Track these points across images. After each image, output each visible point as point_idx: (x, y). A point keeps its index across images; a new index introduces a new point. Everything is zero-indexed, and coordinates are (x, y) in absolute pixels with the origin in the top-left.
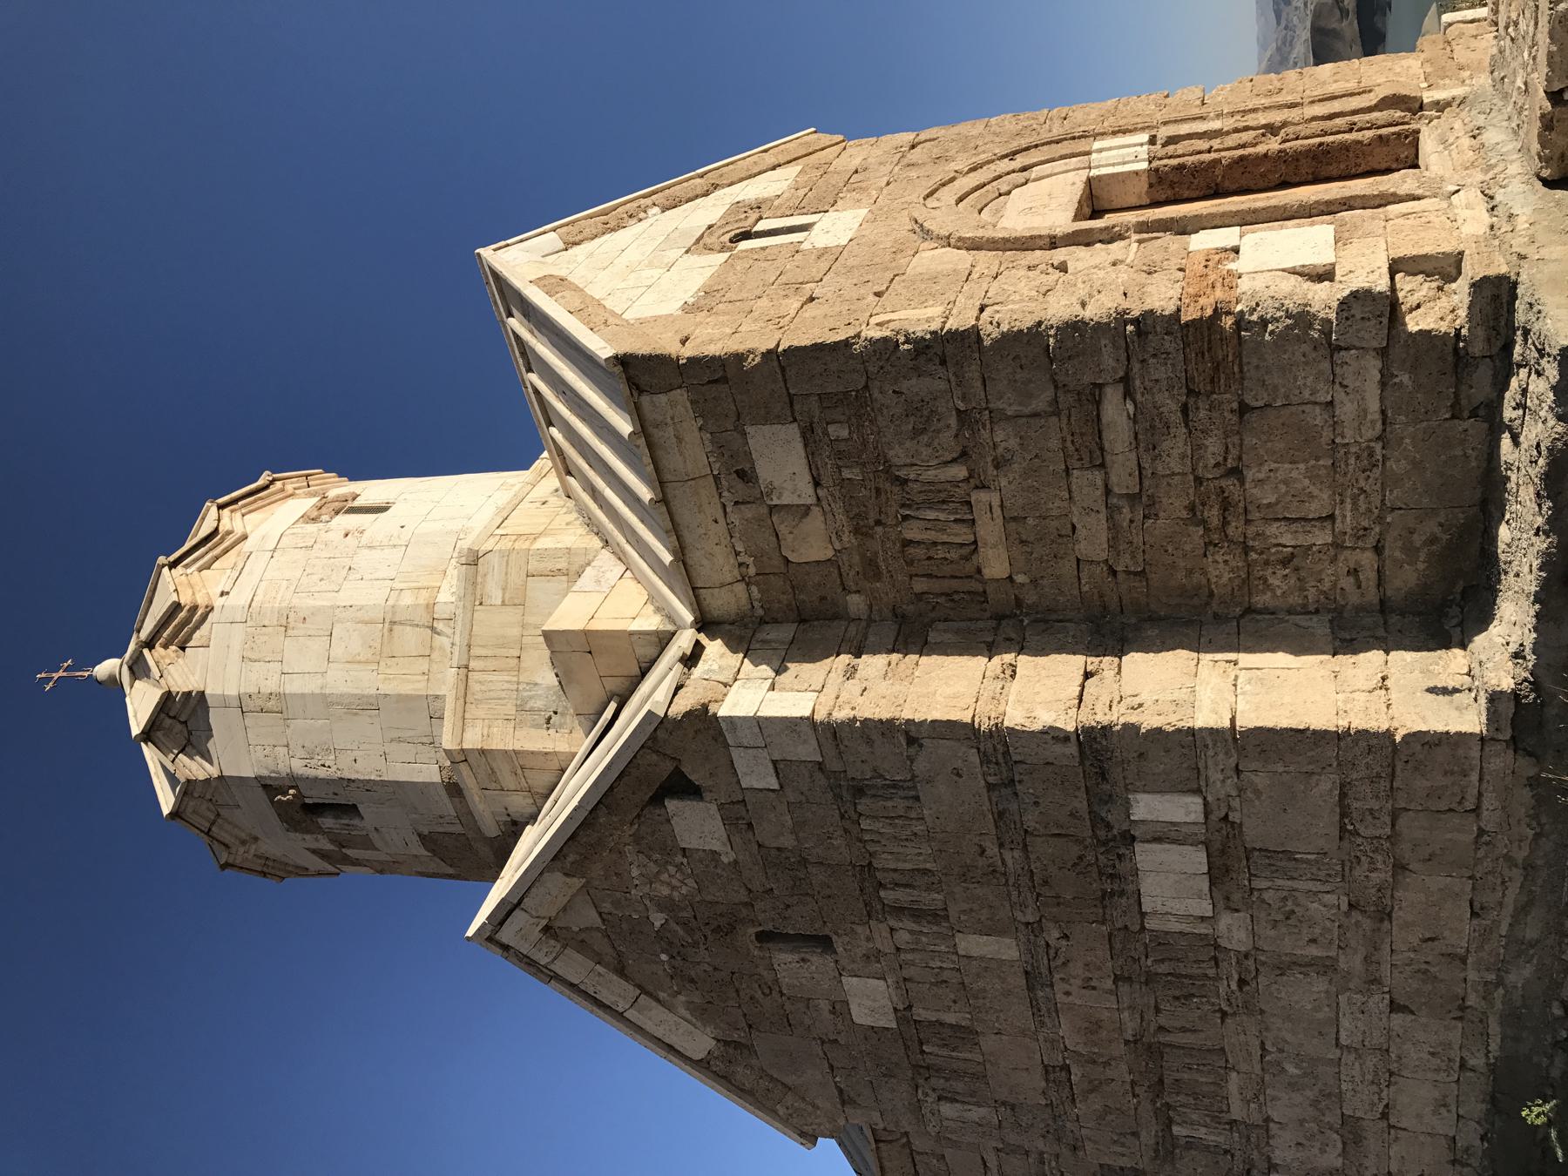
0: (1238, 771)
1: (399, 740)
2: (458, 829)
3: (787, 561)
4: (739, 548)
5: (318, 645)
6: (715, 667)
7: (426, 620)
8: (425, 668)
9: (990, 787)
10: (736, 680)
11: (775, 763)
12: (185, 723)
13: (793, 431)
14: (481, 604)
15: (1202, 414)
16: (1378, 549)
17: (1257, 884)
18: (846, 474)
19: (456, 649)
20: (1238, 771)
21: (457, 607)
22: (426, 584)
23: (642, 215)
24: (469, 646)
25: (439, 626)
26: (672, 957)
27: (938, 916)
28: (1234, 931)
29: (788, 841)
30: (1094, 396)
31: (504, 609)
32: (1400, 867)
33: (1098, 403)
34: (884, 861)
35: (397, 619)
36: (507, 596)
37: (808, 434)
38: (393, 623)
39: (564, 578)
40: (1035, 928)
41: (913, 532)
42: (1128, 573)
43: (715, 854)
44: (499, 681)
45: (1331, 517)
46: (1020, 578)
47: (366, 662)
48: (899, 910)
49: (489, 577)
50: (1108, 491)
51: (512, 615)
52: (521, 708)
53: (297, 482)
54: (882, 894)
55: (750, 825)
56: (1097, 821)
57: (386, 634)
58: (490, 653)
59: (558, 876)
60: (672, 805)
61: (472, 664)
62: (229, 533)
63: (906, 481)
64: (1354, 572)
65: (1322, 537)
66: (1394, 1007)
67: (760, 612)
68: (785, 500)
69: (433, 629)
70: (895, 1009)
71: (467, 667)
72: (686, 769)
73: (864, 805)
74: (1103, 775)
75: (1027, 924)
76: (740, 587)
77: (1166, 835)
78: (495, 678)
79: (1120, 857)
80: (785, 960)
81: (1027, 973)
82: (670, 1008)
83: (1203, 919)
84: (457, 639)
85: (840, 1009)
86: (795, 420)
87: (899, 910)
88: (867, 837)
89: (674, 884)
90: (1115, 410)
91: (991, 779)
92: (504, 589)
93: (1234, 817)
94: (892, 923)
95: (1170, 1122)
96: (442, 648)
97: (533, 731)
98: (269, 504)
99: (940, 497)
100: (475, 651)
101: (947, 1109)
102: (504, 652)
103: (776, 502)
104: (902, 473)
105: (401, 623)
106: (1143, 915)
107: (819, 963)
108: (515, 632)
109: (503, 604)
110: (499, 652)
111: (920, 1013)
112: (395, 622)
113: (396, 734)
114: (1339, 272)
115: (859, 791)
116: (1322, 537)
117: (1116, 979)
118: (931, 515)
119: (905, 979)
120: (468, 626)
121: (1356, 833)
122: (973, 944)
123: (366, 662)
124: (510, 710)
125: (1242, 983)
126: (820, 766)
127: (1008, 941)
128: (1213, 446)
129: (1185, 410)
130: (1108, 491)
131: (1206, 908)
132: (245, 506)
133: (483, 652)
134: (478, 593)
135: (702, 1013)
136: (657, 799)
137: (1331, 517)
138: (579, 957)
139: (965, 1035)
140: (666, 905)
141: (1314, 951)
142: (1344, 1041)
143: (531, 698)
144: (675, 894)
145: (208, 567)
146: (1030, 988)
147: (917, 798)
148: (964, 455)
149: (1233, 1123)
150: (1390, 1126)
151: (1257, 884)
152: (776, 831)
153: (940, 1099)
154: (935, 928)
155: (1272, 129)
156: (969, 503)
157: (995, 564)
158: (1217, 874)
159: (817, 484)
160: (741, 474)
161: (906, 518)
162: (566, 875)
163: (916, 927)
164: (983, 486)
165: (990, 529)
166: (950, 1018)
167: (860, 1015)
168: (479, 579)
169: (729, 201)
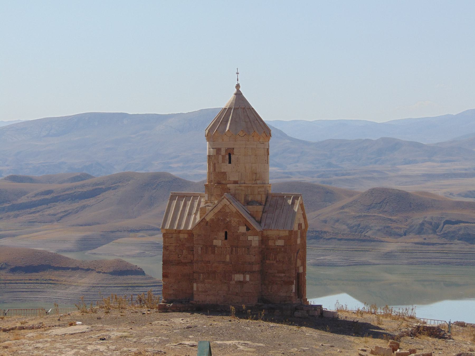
0: (252, 284)
1: (241, 174)
2: (228, 179)
3: (269, 240)
4: (271, 236)
9: (249, 262)
11: (251, 240)
13: (283, 245)
15: (282, 282)
16: (268, 295)
17: (239, 285)
18: (278, 249)
20: (252, 284)
26: (222, 219)
27: (232, 253)
28: (232, 282)
29: (241, 239)
30: (284, 273)
32: (242, 297)
33: (283, 273)
34: (239, 249)
35: (257, 174)
37: (283, 246)
38: (256, 174)
40: (231, 263)
41: (271, 254)
42: (266, 274)
43: (239, 230)
45: (271, 291)
46: (266, 264)
48: (232, 249)
50: (275, 273)
52: (246, 195)
54: (234, 248)
55: (243, 235)
56: (246, 272)
59: (236, 211)
60: (245, 227)
63: (277, 254)
64: (266, 293)
65: (269, 291)
66: (224, 296)
67: (263, 236)
68: (276, 242)
69: (255, 181)
70: (216, 245)
72: (250, 230)
73: (247, 249)
74: (251, 273)
75: (231, 263)
76: (266, 235)
77: (244, 277)
79: (241, 273)
80: (223, 234)
81: (224, 262)
82: (213, 216)
83: (234, 280)
85: (215, 239)
86: (284, 245)
87: (232, 249)
88: (242, 248)
89: (234, 224)
90: (283, 275)
91: (250, 262)
92: (260, 191)
93: (247, 284)
94: (230, 248)
95: (202, 273)
99: (275, 258)
101: (200, 248)
103: (276, 241)
104: (278, 254)
106: (234, 274)
107: (224, 238)
109: (258, 191)
111: (216, 249)
115: (248, 249)
116: (269, 291)
117: (224, 270)
118: (274, 256)
119: (221, 248)
121: (246, 293)
122: (228, 257)
125: (226, 283)
126: (251, 245)
127: (229, 260)
129: (282, 280)
130: (275, 273)
131: (236, 280)
135: (212, 220)
136: (246, 225)
137: (271, 291)
138: (221, 207)
139: (213, 252)
140: (230, 221)
141: (231, 289)
142: (219, 291)
144: (232, 223)
146: (222, 261)
147: (247, 254)
148: (279, 261)
149: (204, 280)
150: (207, 295)
151: (239, 285)
152: (242, 238)
153: (201, 248)
154: (230, 253)
155: (301, 285)
156: (274, 260)
157: (267, 262)
158: (240, 282)
159: (277, 246)
160: (279, 238)
161: (273, 254)
162: (236, 212)
163: (230, 250)
164: (276, 262)
165: (272, 262)
166: (216, 252)
167: (215, 241)
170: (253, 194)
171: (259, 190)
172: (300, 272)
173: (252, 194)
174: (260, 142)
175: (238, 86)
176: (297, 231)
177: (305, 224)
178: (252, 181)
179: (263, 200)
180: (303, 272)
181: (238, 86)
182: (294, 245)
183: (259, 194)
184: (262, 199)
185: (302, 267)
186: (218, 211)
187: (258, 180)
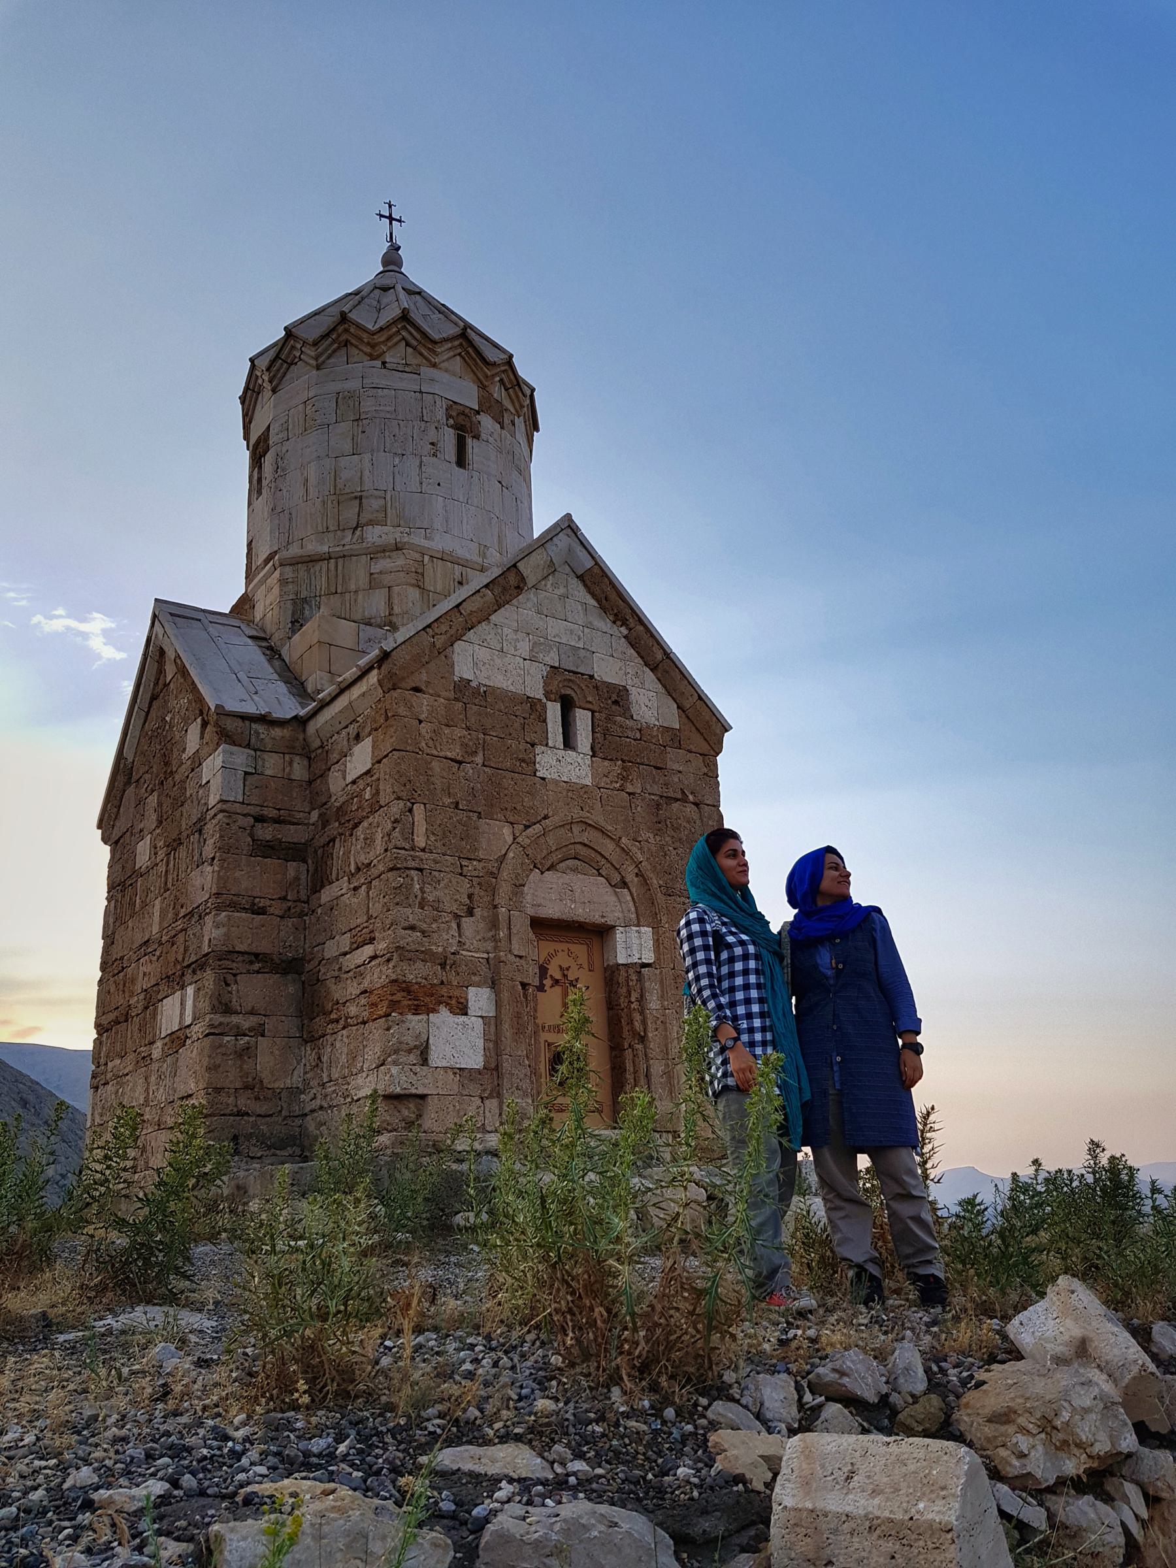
5: (347, 447)
6: (262, 736)
7: (363, 521)
8: (331, 528)
10: (255, 750)
12: (300, 360)
14: (371, 559)
19: (337, 549)
21: (368, 543)
22: (389, 514)
23: (619, 623)
24: (344, 556)
25: (358, 533)
30: (371, 941)
31: (368, 575)
36: (375, 576)
37: (368, 772)
39: (387, 614)
44: (321, 583)
47: (335, 486)
49: (388, 560)
51: (363, 581)
52: (305, 600)
53: (510, 380)
57: (353, 495)
58: (339, 572)
61: (332, 561)
62: (434, 352)
69: (356, 528)
71: (330, 558)
78: (323, 579)
84: (347, 547)
92: (381, 572)
96: (343, 537)
97: (290, 612)
98: (473, 371)
100: (340, 561)
102: (340, 581)
105: (360, 504)
108: (353, 587)
109: (371, 574)
110: (340, 577)
112: (361, 500)
113: (294, 516)
114: (417, 1069)
120: (357, 553)
123: (335, 486)
124: (304, 594)
128: (353, 1010)
132: (468, 352)
133: (340, 568)
134: (379, 555)
138: (154, 672)
143: (311, 607)
145: (408, 344)
155: (643, 1039)
168: (387, 554)
169: (629, 682)
170: (339, 591)
171: (376, 567)
172: (620, 961)
173: (336, 593)
174: (384, 363)
175: (392, 259)
176: (535, 708)
177: (678, 707)
178: (339, 532)
179: (397, 610)
180: (658, 958)
181: (392, 259)
182: (460, 763)
183: (373, 583)
184: (395, 608)
185: (647, 931)
186: (149, 695)
187: (371, 523)
